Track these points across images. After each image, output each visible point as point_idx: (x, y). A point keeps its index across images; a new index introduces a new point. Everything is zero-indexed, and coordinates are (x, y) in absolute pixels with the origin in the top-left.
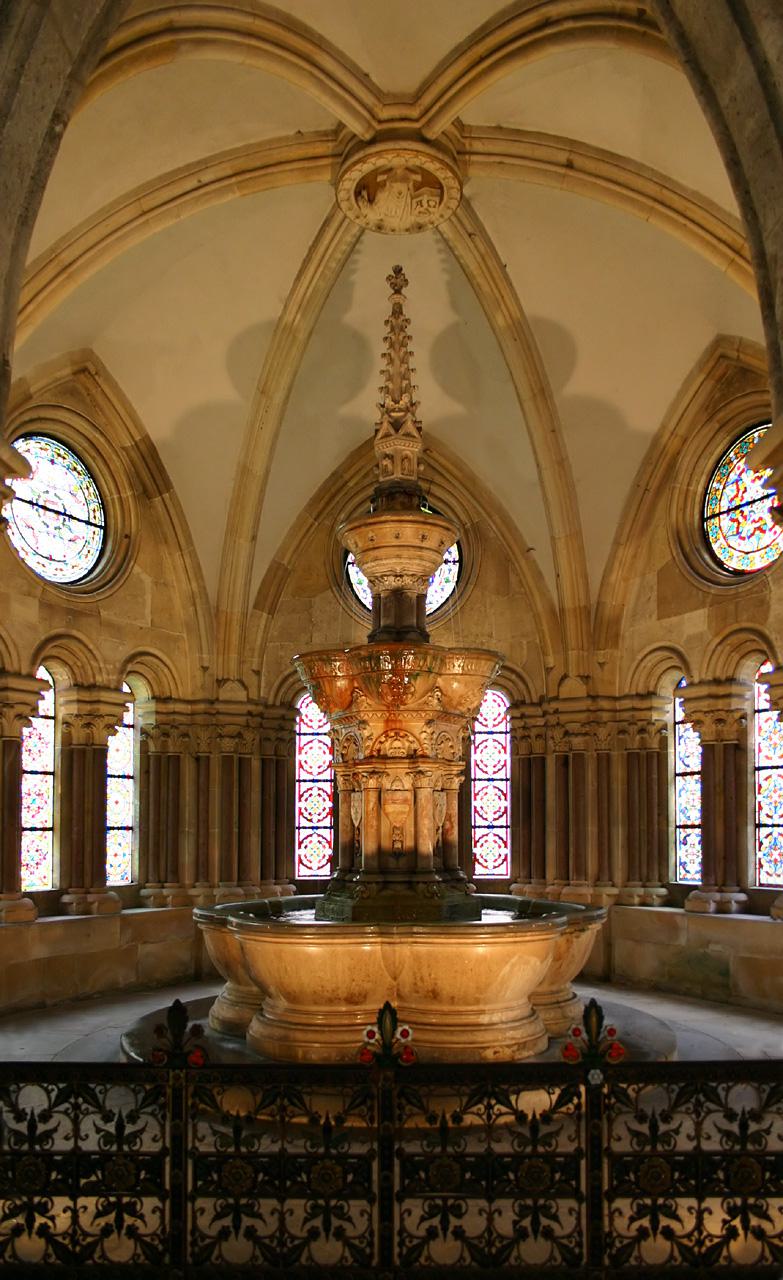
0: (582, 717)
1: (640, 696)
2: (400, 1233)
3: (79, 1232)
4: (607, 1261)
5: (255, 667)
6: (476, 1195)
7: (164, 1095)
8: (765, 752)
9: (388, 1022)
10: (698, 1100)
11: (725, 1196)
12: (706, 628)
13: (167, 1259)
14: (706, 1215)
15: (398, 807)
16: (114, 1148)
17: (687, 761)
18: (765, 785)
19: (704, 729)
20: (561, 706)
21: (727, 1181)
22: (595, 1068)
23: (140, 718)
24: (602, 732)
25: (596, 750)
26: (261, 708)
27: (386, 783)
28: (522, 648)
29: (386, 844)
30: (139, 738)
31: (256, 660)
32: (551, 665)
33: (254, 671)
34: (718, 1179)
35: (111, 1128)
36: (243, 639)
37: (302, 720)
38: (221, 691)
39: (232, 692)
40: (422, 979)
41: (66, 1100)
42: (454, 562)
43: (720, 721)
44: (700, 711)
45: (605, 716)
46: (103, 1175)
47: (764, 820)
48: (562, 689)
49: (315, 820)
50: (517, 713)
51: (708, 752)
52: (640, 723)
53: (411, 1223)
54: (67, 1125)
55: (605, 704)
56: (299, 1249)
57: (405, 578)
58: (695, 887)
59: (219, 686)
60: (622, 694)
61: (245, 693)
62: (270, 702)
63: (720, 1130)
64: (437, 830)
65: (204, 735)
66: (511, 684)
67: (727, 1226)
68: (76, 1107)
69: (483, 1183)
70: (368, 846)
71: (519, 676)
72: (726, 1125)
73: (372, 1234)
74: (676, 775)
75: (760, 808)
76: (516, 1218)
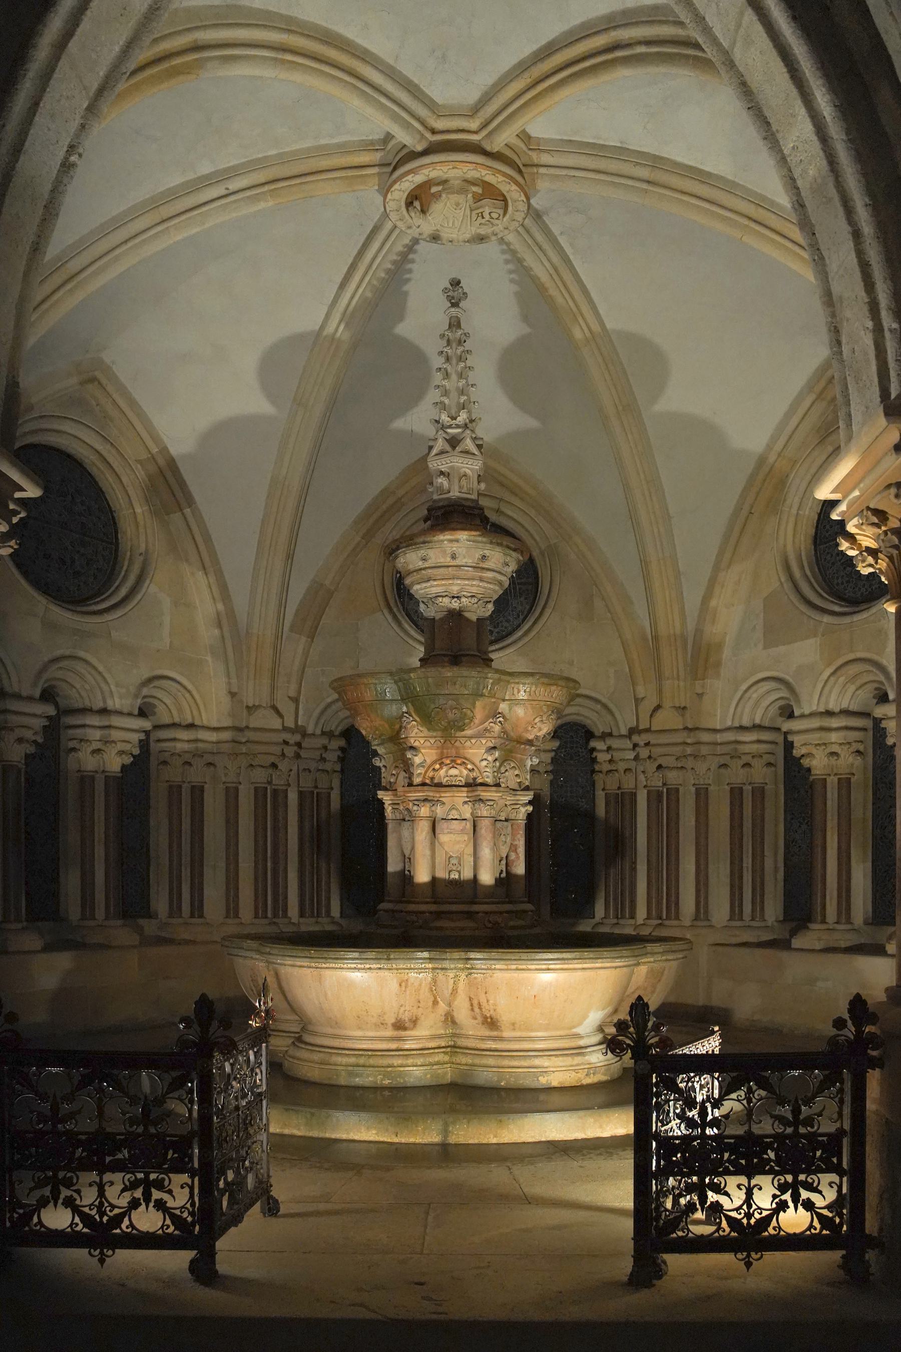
0: (677, 750)
3: (106, 1204)
5: (292, 694)
11: (776, 1173)
14: (755, 1190)
21: (778, 1160)
27: (440, 811)
31: (293, 687)
34: (770, 1160)
39: (266, 720)
45: (704, 750)
48: (654, 720)
52: (743, 757)
55: (705, 737)
59: (250, 714)
61: (279, 721)
67: (777, 1200)
71: (605, 706)
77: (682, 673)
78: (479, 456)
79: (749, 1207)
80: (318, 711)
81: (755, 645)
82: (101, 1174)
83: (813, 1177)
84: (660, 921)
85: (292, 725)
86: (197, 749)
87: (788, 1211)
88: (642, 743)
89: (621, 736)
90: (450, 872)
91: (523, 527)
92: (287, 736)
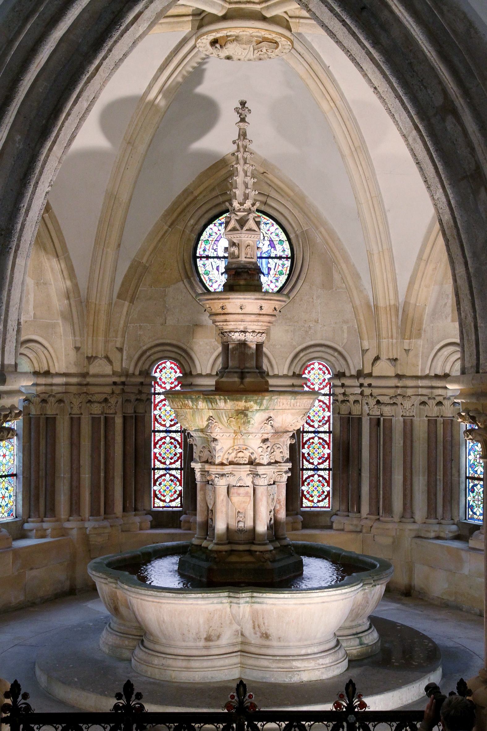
0: (391, 392)
1: (437, 377)
5: (118, 345)
15: (241, 498)
20: (374, 383)
24: (407, 404)
25: (402, 416)
26: (123, 379)
27: (232, 481)
28: (343, 331)
29: (233, 525)
31: (119, 339)
32: (367, 348)
33: (117, 348)
36: (109, 323)
38: (91, 367)
40: (259, 626)
45: (410, 392)
49: (168, 463)
50: (338, 382)
52: (436, 398)
57: (247, 334)
59: (89, 363)
60: (424, 374)
61: (110, 367)
62: (131, 371)
64: (270, 512)
65: (76, 402)
66: (334, 359)
70: (220, 526)
71: (340, 353)
77: (395, 335)
85: (119, 370)
88: (366, 384)
89: (352, 376)
90: (239, 522)
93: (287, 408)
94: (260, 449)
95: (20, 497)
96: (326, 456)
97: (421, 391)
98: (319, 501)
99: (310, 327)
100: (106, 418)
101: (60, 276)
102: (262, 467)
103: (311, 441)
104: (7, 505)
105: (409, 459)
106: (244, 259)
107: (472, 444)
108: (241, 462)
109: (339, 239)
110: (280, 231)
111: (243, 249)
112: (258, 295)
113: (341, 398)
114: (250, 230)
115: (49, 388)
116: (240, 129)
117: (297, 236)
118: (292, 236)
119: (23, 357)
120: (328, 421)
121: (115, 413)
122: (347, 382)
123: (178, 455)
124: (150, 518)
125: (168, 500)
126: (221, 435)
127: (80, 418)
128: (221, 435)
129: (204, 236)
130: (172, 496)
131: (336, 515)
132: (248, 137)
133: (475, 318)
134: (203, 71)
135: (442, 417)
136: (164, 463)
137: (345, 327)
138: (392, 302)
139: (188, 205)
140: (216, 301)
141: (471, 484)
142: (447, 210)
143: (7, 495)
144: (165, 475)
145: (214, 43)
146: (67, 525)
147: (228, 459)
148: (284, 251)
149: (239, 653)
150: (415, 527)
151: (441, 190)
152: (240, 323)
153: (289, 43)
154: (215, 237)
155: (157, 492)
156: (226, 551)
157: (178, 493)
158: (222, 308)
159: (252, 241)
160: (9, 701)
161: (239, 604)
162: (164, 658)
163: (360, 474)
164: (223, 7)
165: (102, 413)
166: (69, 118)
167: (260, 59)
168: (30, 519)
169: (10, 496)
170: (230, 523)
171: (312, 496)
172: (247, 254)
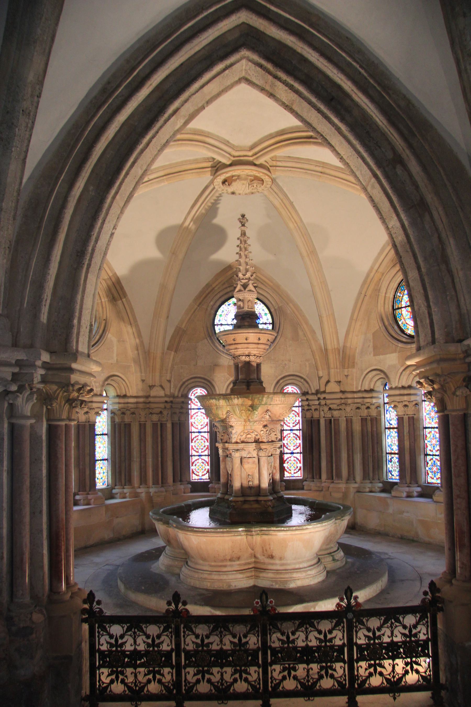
0: (338, 402)
1: (366, 391)
2: (271, 678)
3: (138, 682)
4: (356, 686)
5: (168, 378)
6: (302, 663)
7: (171, 628)
8: (428, 420)
9: (264, 597)
10: (392, 622)
11: (403, 658)
12: (397, 362)
13: (175, 691)
14: (396, 666)
16: (151, 649)
17: (391, 422)
18: (428, 435)
19: (398, 409)
20: (327, 396)
22: (350, 612)
23: (111, 406)
24: (348, 409)
25: (345, 417)
26: (171, 399)
27: (244, 454)
29: (245, 484)
30: (110, 415)
31: (169, 375)
33: (167, 380)
34: (401, 652)
35: (150, 641)
36: (162, 366)
37: (192, 402)
40: (266, 550)
41: (131, 630)
42: (270, 324)
43: (406, 406)
44: (396, 401)
45: (350, 401)
46: (147, 659)
47: (429, 452)
48: (326, 388)
50: (304, 398)
51: (400, 420)
52: (366, 404)
53: (275, 675)
54: (131, 641)
56: (229, 687)
58: (396, 484)
60: (357, 390)
62: (176, 395)
63: (401, 633)
67: (404, 669)
68: (135, 633)
69: (305, 658)
70: (237, 484)
71: (305, 380)
72: (403, 631)
73: (259, 680)
74: (386, 428)
75: (427, 446)
76: (319, 671)
77: (338, 367)
78: (256, 292)
79: (394, 673)
80: (179, 385)
81: (370, 354)
82: (135, 669)
83: (419, 659)
84: (332, 481)
85: (169, 394)
86: (128, 407)
87: (409, 674)
88: (322, 398)
89: (313, 394)
90: (249, 481)
91: (267, 299)
92: (167, 399)
93: (279, 403)
94: (262, 432)
95: (110, 473)
96: (298, 445)
97: (356, 401)
98: (295, 473)
99: (285, 365)
100: (161, 424)
101: (132, 336)
102: (264, 444)
103: (289, 435)
104: (102, 478)
105: (351, 443)
106: (247, 309)
107: (389, 432)
108: (249, 441)
109: (301, 310)
110: (265, 308)
111: (246, 303)
112: (256, 331)
113: (306, 408)
114: (250, 291)
115: (126, 405)
116: (242, 231)
117: (275, 310)
118: (272, 310)
119: (110, 386)
120: (299, 423)
121: (167, 421)
122: (310, 397)
123: (206, 447)
124: (190, 486)
125: (201, 475)
126: (236, 423)
127: (145, 424)
128: (236, 423)
129: (219, 312)
130: (203, 472)
131: (306, 481)
132: (247, 235)
133: (429, 307)
134: (217, 209)
135: (370, 416)
136: (198, 452)
137: (307, 363)
138: (336, 347)
139: (209, 293)
140: (230, 335)
141: (390, 457)
142: (401, 232)
143: (102, 472)
144: (198, 459)
145: (224, 182)
146: (139, 490)
147: (240, 439)
148: (268, 319)
149: (253, 569)
150: (356, 485)
151: (395, 218)
152: (246, 349)
153: (270, 180)
154: (225, 312)
155: (194, 470)
156: (241, 501)
157: (207, 470)
158: (234, 340)
159: (252, 298)
160: (86, 606)
161: (252, 535)
162: (202, 573)
163: (320, 453)
164: (229, 159)
165: (159, 421)
166: (128, 176)
167: (252, 193)
168: (116, 487)
169: (104, 473)
170: (243, 482)
171: (290, 470)
172: (248, 306)
